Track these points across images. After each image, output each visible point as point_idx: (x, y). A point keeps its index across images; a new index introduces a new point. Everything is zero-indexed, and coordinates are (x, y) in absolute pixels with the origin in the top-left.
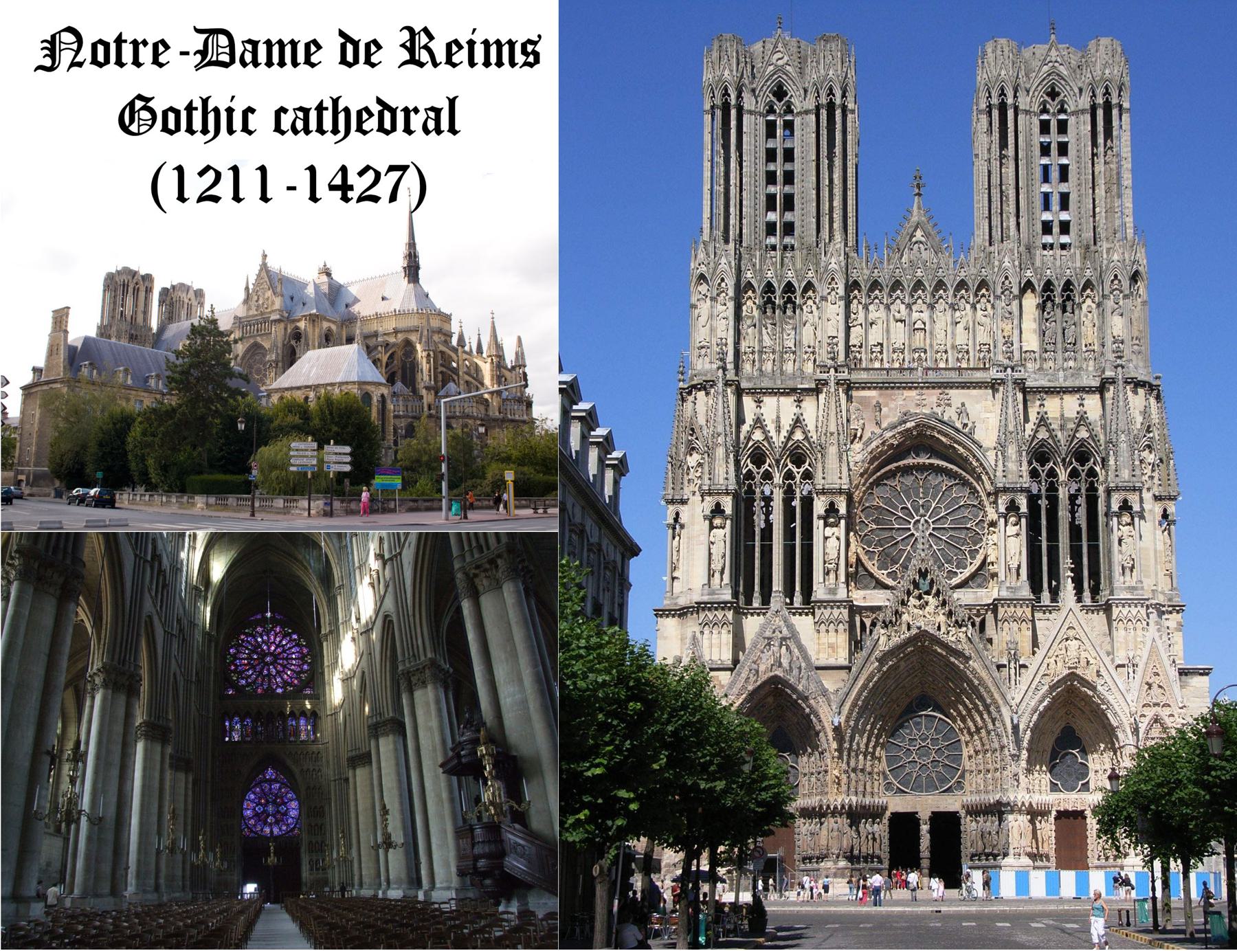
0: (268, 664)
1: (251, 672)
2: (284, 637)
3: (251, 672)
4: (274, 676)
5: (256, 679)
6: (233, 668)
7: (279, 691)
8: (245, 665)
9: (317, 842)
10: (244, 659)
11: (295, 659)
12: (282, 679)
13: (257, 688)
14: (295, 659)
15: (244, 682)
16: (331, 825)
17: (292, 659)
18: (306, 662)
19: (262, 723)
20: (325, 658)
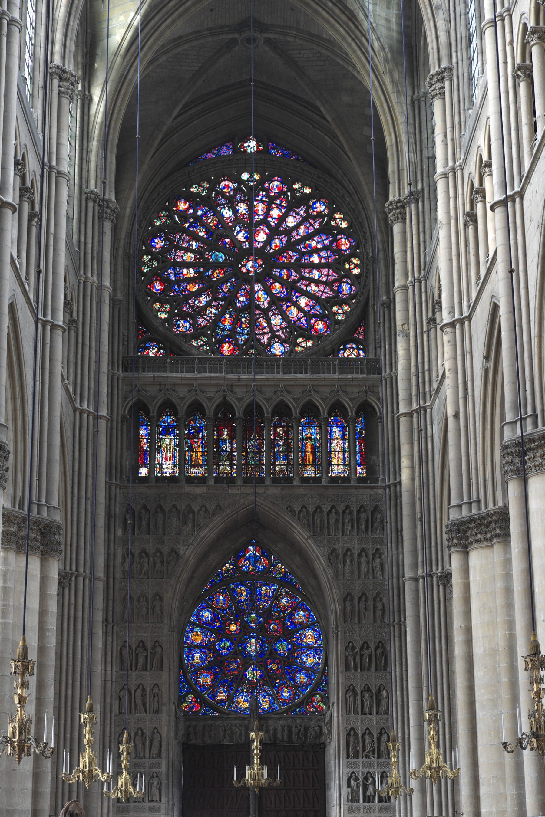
0: (247, 279)
1: (204, 299)
2: (290, 209)
3: (204, 299)
4: (265, 312)
5: (220, 317)
6: (158, 286)
7: (278, 349)
8: (191, 281)
9: (368, 731)
10: (188, 265)
11: (319, 267)
12: (285, 317)
13: (221, 342)
14: (319, 267)
15: (184, 326)
16: (404, 690)
17: (313, 266)
18: (348, 274)
19: (232, 436)
20: (398, 267)
